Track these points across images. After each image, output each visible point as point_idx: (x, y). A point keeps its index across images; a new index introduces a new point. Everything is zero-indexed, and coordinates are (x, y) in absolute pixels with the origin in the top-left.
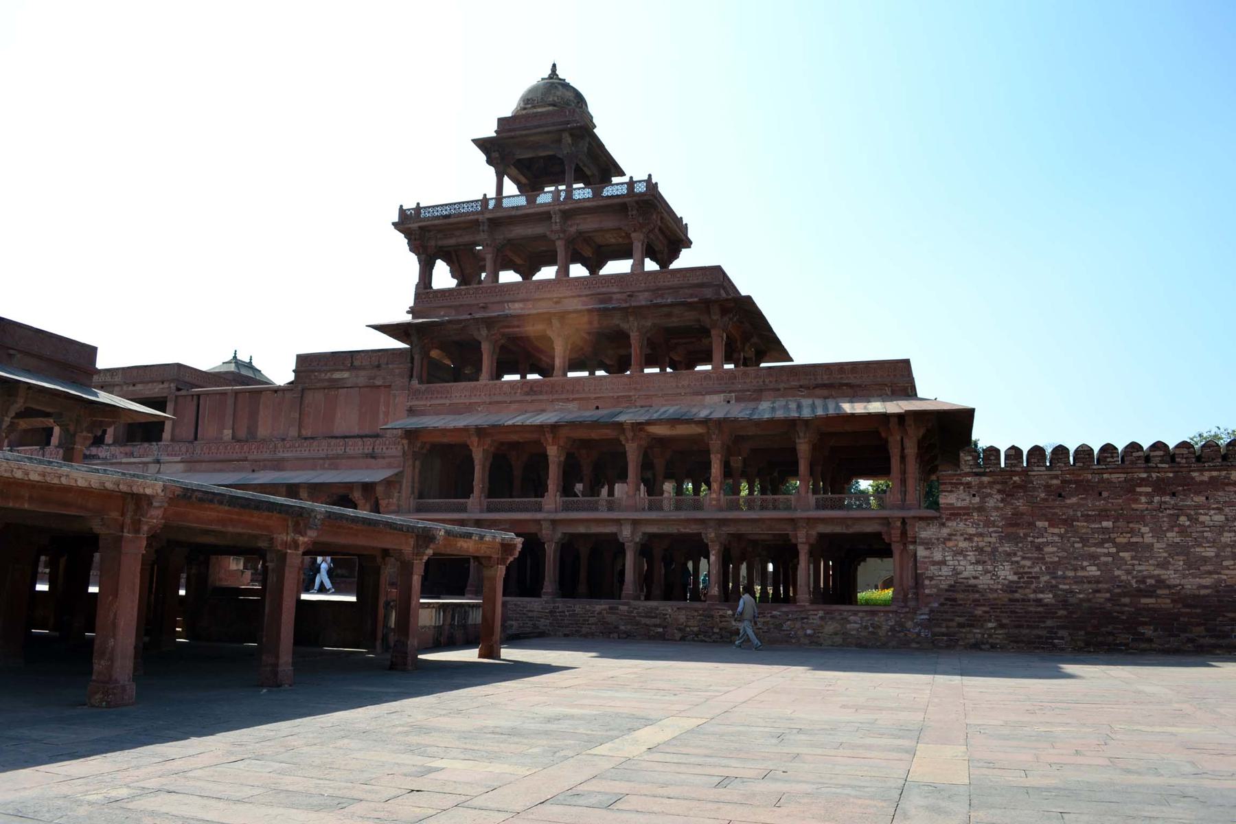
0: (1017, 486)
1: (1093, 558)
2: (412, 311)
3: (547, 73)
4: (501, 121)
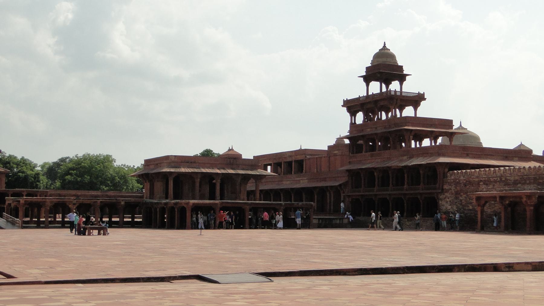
0: (458, 183)
1: (471, 203)
2: (350, 132)
3: (381, 47)
4: (367, 68)
